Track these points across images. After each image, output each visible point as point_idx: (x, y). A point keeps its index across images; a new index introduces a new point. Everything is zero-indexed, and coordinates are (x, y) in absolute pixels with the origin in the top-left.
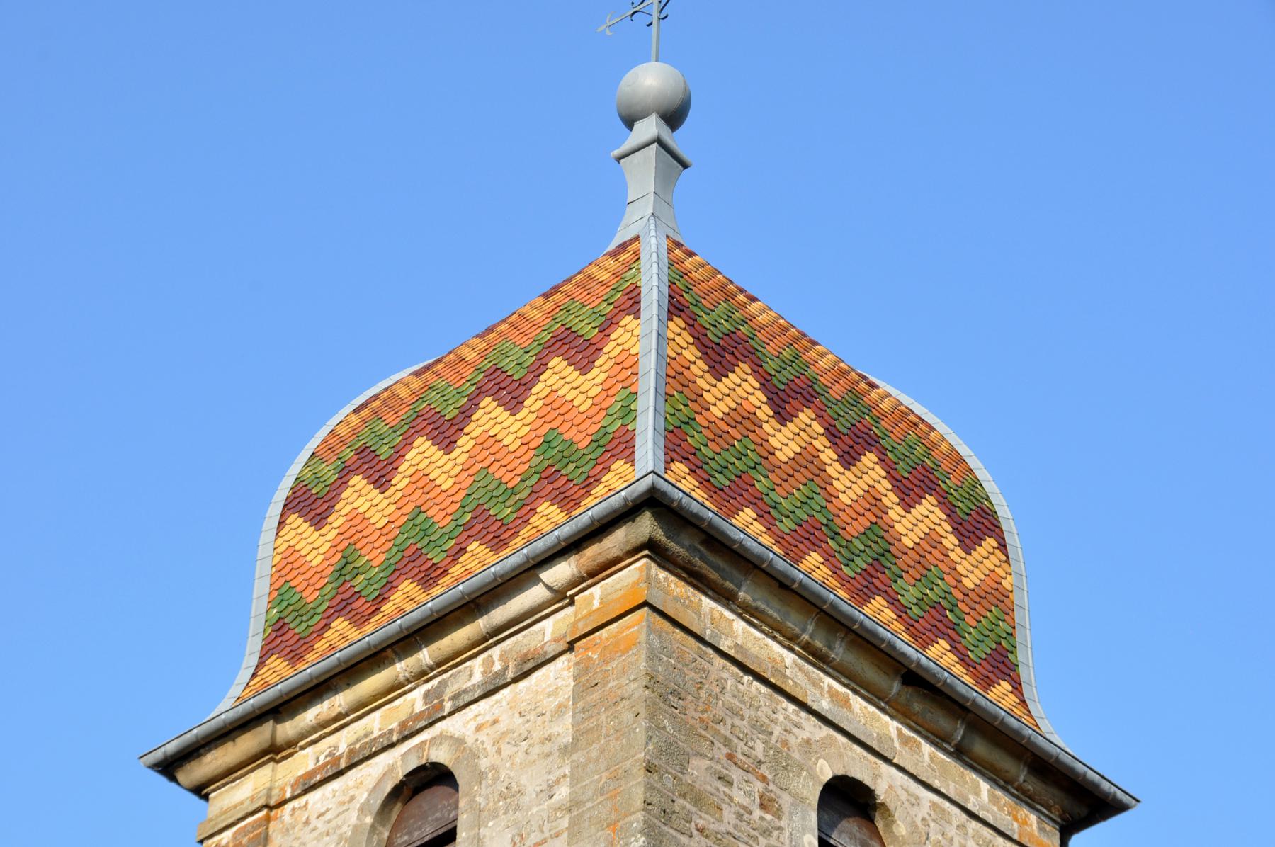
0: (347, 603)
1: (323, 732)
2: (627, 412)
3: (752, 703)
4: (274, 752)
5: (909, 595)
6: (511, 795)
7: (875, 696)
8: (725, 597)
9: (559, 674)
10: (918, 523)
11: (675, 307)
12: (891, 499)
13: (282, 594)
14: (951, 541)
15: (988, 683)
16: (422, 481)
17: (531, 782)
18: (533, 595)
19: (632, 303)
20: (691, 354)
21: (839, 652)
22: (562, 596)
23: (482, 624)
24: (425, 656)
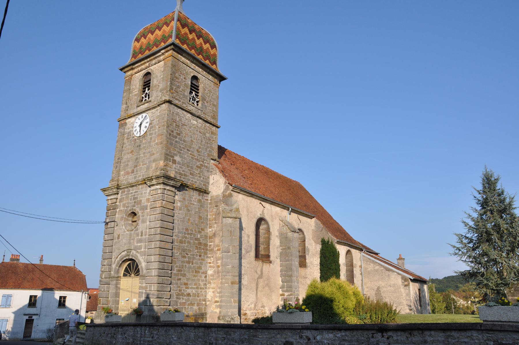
0: (141, 52)
1: (139, 67)
2: (172, 33)
3: (184, 67)
4: (132, 69)
5: (204, 55)
6: (157, 76)
7: (199, 66)
8: (181, 55)
9: (162, 63)
10: (206, 46)
11: (178, 20)
12: (203, 43)
13: (134, 51)
14: (210, 48)
15: (212, 65)
16: (149, 39)
17: (159, 75)
18: (160, 54)
19: (173, 20)
20: (180, 26)
21: (195, 61)
22: (163, 54)
23: (154, 56)
24: (148, 59)
